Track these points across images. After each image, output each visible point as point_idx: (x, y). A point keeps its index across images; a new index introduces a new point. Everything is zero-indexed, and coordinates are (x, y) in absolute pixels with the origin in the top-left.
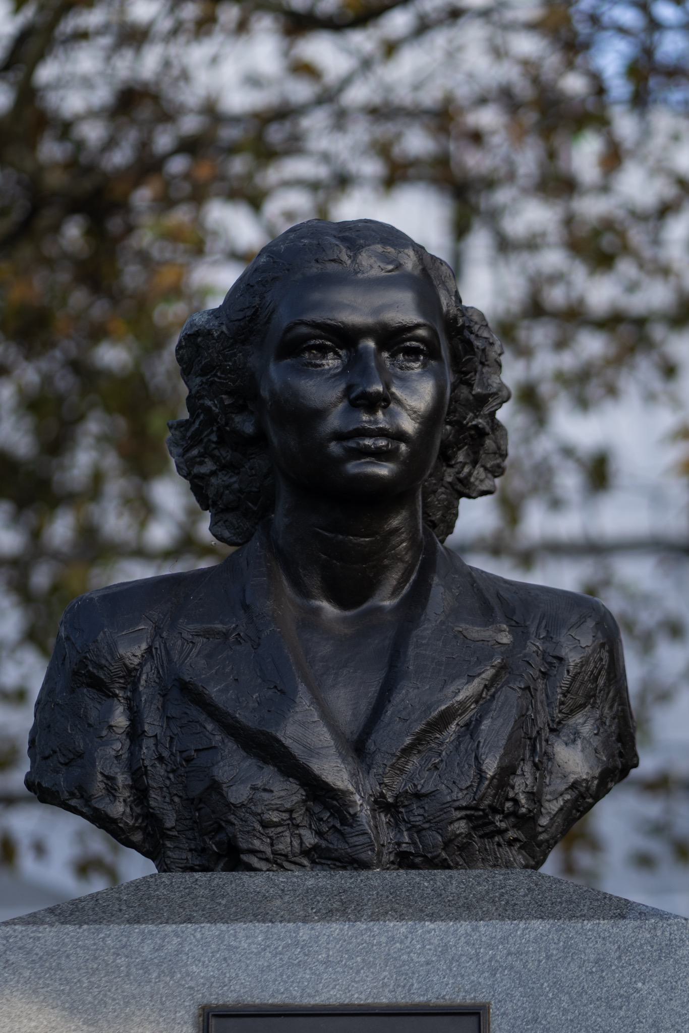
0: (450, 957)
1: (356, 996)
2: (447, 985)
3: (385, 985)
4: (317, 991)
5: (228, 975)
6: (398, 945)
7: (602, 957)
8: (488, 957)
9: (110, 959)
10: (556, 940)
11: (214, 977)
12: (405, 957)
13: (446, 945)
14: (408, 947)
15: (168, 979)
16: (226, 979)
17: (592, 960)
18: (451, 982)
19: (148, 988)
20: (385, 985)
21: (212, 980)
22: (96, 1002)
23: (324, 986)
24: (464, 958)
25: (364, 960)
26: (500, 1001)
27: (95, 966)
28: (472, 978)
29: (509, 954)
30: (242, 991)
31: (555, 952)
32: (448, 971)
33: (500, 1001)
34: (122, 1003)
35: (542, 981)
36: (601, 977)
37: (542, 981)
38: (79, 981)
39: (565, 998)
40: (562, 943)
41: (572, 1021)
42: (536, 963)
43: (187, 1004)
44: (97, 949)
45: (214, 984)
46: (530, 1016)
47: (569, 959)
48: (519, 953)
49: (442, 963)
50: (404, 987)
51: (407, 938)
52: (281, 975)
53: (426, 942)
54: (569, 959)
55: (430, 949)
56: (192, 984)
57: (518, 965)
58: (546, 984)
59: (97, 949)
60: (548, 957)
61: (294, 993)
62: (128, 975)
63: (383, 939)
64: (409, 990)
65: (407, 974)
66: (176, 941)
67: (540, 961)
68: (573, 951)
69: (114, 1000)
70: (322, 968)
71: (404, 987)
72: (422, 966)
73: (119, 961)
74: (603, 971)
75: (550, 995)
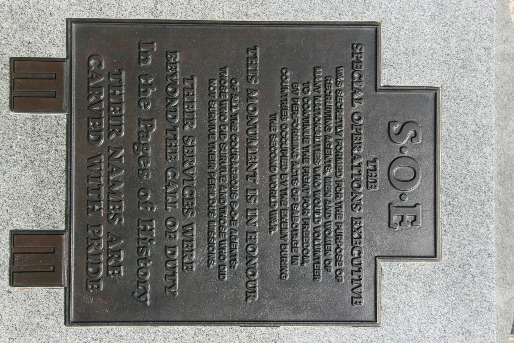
0: (471, 239)
1: (447, 181)
2: (454, 237)
3: (454, 199)
4: (450, 157)
5: (461, 102)
6: (479, 207)
7: (472, 334)
8: (471, 262)
9: (473, 28)
10: (482, 306)
11: (460, 94)
12: (471, 211)
13: (479, 237)
14: (478, 213)
15: (460, 65)
16: (458, 101)
17: (470, 328)
18: (455, 239)
19: (454, 52)
20: (454, 199)
21: (458, 93)
22: (445, 20)
23: (453, 161)
24: (471, 248)
25: (470, 186)
26: (443, 270)
27: (469, 19)
28: (458, 253)
29: (474, 276)
30: (451, 111)
31: (474, 305)
32: (462, 238)
33: (443, 270)
34: (445, 36)
35: (456, 296)
36: (459, 334)
37: (456, 296)
38: (459, 9)
39: (445, 311)
40: (480, 309)
41: (431, 314)
42: (468, 293)
43: (443, 76)
44: (480, 20)
45: (455, 94)
46: (434, 288)
47: (470, 314)
48: (474, 283)
49: (468, 235)
50: (453, 211)
51: (484, 213)
52: (460, 135)
53: (481, 225)
54: (470, 314)
55: (476, 227)
56: (456, 80)
57: (466, 282)
58: (454, 298)
59: (480, 20)
60: (471, 301)
61: (449, 143)
62: (463, 40)
63: (483, 198)
64: (450, 214)
65: (460, 212)
66: (484, 69)
67: (469, 295)
68: (476, 316)
69: (447, 31)
70: (465, 160)
71: (453, 211)
72: (466, 222)
73: (471, 34)
74: (463, 334)
75: (447, 301)
